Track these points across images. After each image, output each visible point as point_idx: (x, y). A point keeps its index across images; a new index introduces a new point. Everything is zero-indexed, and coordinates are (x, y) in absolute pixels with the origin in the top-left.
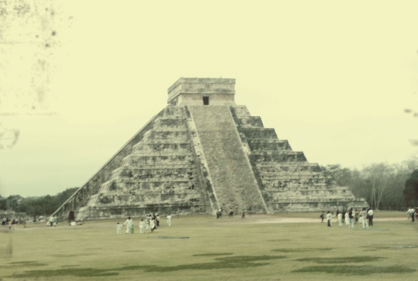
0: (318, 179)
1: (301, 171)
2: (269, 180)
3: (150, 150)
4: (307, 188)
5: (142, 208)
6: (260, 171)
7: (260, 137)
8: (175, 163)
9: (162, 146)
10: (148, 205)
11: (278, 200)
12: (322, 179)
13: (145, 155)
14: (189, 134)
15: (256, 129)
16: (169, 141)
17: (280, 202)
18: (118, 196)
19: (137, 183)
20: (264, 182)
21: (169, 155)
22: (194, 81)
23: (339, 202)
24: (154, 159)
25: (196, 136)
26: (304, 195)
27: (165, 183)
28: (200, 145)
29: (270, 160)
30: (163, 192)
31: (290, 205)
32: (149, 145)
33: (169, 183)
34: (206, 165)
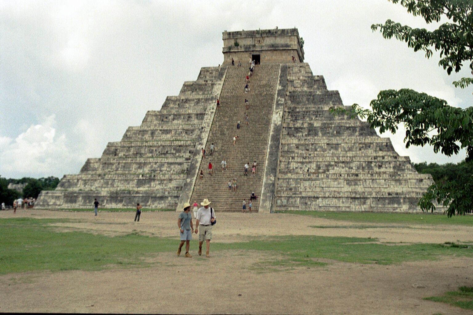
0: (382, 162)
1: (360, 150)
2: (302, 163)
3: (155, 122)
4: (357, 175)
5: (104, 196)
9: (171, 117)
10: (112, 193)
11: (301, 193)
12: (390, 163)
15: (310, 92)
16: (182, 111)
17: (304, 194)
18: (82, 180)
22: (239, 36)
23: (404, 198)
26: (350, 185)
27: (152, 164)
28: (214, 114)
29: (316, 134)
30: (141, 176)
31: (320, 200)
33: (158, 164)
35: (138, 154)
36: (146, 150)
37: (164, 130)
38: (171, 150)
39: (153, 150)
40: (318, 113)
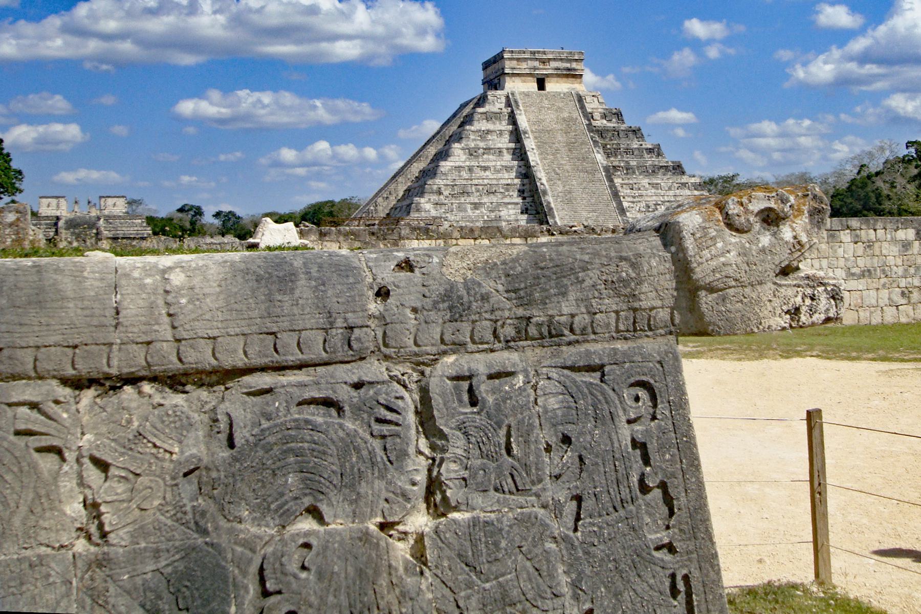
2: (633, 202)
3: (463, 158)
6: (619, 188)
8: (500, 175)
9: (481, 151)
13: (457, 164)
14: (517, 135)
20: (625, 204)
21: (490, 164)
24: (470, 169)
32: (463, 149)
35: (464, 193)
40: (628, 151)
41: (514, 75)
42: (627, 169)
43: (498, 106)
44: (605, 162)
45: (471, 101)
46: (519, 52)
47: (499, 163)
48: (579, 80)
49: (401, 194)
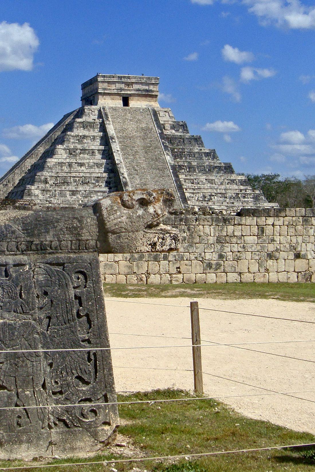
1: (228, 184)
2: (193, 193)
4: (233, 203)
6: (183, 182)
7: (184, 144)
13: (60, 161)
14: (106, 140)
19: (53, 191)
20: (187, 195)
21: (85, 161)
24: (70, 165)
25: (115, 142)
28: (119, 152)
30: (80, 202)
32: (65, 149)
34: (126, 175)
35: (65, 182)
36: (72, 179)
37: (78, 163)
38: (91, 180)
39: (76, 180)
41: (105, 94)
42: (189, 168)
43: (93, 117)
44: (173, 162)
45: (72, 113)
46: (110, 77)
47: (91, 161)
48: (154, 99)
49: (17, 182)
